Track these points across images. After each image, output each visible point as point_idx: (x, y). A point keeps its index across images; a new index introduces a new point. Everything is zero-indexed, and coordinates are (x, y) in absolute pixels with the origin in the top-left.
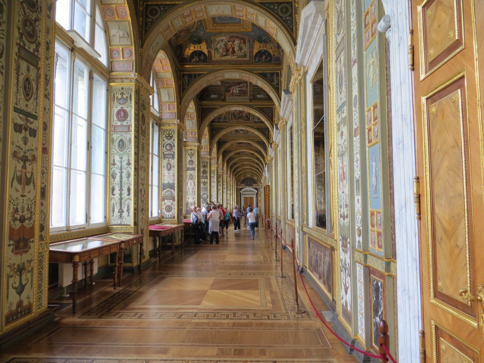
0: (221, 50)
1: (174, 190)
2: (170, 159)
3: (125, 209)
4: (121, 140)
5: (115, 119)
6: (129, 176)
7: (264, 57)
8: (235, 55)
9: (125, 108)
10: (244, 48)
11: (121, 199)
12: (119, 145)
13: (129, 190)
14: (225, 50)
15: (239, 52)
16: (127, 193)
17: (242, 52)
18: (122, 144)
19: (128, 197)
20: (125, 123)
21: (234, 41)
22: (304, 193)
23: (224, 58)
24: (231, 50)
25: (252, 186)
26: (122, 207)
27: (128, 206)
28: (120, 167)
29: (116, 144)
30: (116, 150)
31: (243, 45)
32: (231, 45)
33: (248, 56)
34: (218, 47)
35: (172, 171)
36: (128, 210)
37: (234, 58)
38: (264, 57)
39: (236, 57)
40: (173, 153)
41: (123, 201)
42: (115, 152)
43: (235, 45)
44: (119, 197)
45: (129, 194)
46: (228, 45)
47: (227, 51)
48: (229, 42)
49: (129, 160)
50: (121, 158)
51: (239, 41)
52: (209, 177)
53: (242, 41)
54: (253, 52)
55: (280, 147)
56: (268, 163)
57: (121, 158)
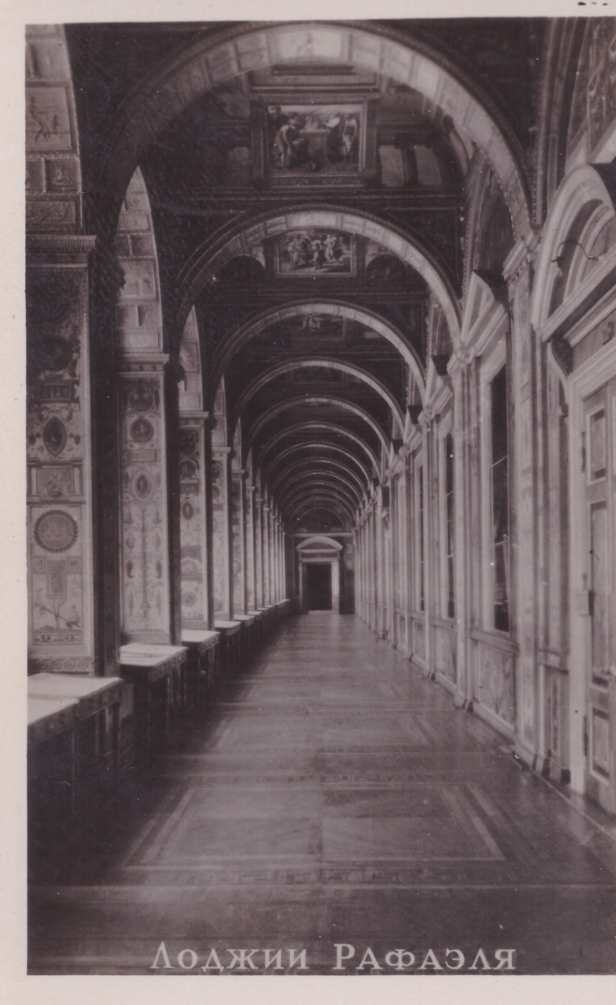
0: (295, 257)
1: (200, 561)
2: (191, 495)
3: (153, 603)
4: (142, 478)
5: (129, 437)
6: (158, 542)
7: (388, 271)
8: (325, 265)
9: (147, 417)
10: (345, 251)
11: (145, 584)
12: (138, 486)
13: (159, 567)
14: (304, 254)
15: (334, 260)
16: (156, 574)
17: (341, 259)
18: (143, 486)
19: (158, 580)
20: (147, 446)
21: (324, 238)
22: (476, 572)
23: (302, 273)
24: (316, 255)
25: (328, 531)
26: (148, 598)
27: (159, 598)
28: (141, 526)
29: (133, 484)
30: (134, 496)
31: (344, 248)
32: (317, 245)
33: (353, 266)
34: (290, 249)
35: (194, 521)
36: (159, 605)
37: (320, 272)
38: (388, 271)
39: (326, 269)
40: (195, 482)
41: (148, 587)
42: (131, 498)
43: (326, 246)
44: (141, 580)
45: (160, 576)
46: (311, 246)
47: (309, 257)
48: (314, 239)
49: (158, 514)
50: (143, 511)
51: (335, 239)
52: (241, 521)
53: (341, 238)
54: (363, 260)
55: (422, 458)
56: (381, 480)
57: (143, 511)
